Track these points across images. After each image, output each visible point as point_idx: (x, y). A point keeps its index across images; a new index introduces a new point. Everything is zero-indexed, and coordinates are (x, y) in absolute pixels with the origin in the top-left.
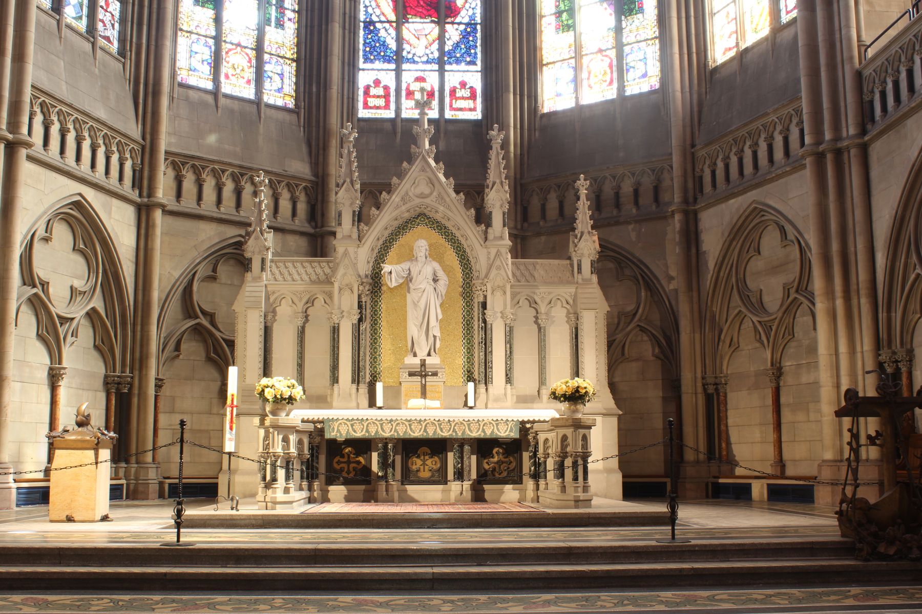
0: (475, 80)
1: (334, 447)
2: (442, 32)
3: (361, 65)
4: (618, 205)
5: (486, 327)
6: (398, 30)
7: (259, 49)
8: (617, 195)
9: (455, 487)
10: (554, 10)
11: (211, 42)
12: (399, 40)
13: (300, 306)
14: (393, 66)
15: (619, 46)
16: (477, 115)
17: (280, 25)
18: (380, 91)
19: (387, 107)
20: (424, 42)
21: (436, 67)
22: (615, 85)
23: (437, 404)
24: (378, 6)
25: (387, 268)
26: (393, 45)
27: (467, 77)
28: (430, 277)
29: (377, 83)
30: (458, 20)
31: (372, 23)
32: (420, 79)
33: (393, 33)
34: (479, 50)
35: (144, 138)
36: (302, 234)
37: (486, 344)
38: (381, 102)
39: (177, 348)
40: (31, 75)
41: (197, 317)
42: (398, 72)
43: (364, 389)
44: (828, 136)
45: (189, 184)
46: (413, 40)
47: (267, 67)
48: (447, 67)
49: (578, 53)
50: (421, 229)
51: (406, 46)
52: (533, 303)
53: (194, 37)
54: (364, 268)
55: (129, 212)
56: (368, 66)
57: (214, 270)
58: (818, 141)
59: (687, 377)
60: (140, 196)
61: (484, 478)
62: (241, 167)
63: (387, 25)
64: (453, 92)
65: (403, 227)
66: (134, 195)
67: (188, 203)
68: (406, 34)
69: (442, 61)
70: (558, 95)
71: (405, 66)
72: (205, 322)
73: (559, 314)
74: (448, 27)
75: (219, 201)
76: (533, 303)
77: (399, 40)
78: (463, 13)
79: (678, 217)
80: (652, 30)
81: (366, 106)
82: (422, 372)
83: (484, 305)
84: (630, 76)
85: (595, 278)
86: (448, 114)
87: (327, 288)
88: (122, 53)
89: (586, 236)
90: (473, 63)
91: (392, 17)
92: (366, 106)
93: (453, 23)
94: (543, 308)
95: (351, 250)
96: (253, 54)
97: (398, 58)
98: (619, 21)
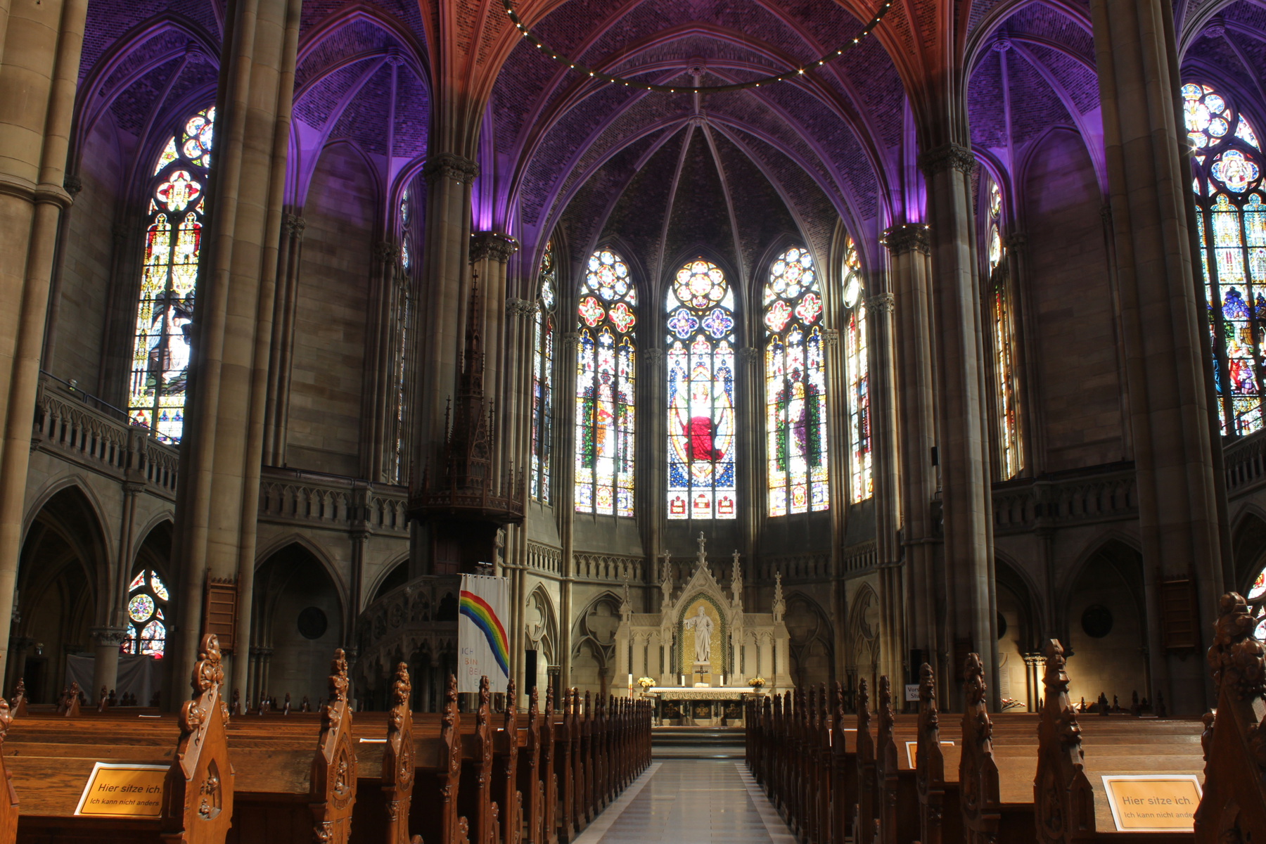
0: (733, 496)
1: (665, 703)
2: (714, 468)
3: (669, 488)
4: (807, 573)
5: (731, 648)
6: (689, 467)
7: (615, 486)
8: (806, 568)
9: (714, 719)
10: (775, 457)
11: (590, 486)
12: (690, 473)
13: (645, 637)
14: (686, 489)
15: (809, 482)
16: (733, 516)
17: (625, 470)
18: (680, 503)
19: (683, 512)
20: (703, 474)
21: (710, 489)
22: (806, 505)
23: (707, 685)
24: (678, 454)
25: (685, 621)
26: (686, 477)
27: (727, 494)
28: (705, 624)
29: (678, 498)
30: (722, 461)
31: (675, 464)
32: (702, 496)
33: (686, 469)
34: (734, 478)
35: (562, 546)
36: (639, 587)
37: (732, 654)
38: (680, 510)
39: (579, 650)
40: (527, 535)
41: (588, 635)
42: (690, 492)
43: (675, 676)
44: (886, 561)
45: (583, 566)
46: (698, 474)
47: (619, 495)
48: (717, 489)
50: (702, 601)
51: (694, 477)
52: (754, 634)
53: (582, 485)
54: (675, 620)
55: (556, 585)
56: (673, 489)
57: (595, 609)
58: (882, 562)
59: (837, 666)
60: (562, 576)
61: (726, 716)
62: (608, 554)
63: (683, 465)
64: (720, 503)
65: (693, 599)
66: (558, 576)
67: (583, 577)
68: (694, 470)
70: (778, 507)
71: (693, 489)
72: (592, 637)
73: (767, 639)
74: (717, 465)
75: (597, 574)
76: (754, 634)
77: (690, 473)
78: (725, 457)
79: (834, 583)
80: (825, 477)
81: (672, 512)
82: (701, 671)
83: (730, 637)
84: (815, 500)
85: (783, 623)
86: (718, 516)
87: (658, 628)
88: (551, 503)
89: (779, 602)
90: (731, 486)
91: (686, 460)
92: (672, 512)
93: (720, 463)
94: (758, 637)
95: (669, 612)
96: (611, 489)
97: (690, 484)
98: (809, 468)
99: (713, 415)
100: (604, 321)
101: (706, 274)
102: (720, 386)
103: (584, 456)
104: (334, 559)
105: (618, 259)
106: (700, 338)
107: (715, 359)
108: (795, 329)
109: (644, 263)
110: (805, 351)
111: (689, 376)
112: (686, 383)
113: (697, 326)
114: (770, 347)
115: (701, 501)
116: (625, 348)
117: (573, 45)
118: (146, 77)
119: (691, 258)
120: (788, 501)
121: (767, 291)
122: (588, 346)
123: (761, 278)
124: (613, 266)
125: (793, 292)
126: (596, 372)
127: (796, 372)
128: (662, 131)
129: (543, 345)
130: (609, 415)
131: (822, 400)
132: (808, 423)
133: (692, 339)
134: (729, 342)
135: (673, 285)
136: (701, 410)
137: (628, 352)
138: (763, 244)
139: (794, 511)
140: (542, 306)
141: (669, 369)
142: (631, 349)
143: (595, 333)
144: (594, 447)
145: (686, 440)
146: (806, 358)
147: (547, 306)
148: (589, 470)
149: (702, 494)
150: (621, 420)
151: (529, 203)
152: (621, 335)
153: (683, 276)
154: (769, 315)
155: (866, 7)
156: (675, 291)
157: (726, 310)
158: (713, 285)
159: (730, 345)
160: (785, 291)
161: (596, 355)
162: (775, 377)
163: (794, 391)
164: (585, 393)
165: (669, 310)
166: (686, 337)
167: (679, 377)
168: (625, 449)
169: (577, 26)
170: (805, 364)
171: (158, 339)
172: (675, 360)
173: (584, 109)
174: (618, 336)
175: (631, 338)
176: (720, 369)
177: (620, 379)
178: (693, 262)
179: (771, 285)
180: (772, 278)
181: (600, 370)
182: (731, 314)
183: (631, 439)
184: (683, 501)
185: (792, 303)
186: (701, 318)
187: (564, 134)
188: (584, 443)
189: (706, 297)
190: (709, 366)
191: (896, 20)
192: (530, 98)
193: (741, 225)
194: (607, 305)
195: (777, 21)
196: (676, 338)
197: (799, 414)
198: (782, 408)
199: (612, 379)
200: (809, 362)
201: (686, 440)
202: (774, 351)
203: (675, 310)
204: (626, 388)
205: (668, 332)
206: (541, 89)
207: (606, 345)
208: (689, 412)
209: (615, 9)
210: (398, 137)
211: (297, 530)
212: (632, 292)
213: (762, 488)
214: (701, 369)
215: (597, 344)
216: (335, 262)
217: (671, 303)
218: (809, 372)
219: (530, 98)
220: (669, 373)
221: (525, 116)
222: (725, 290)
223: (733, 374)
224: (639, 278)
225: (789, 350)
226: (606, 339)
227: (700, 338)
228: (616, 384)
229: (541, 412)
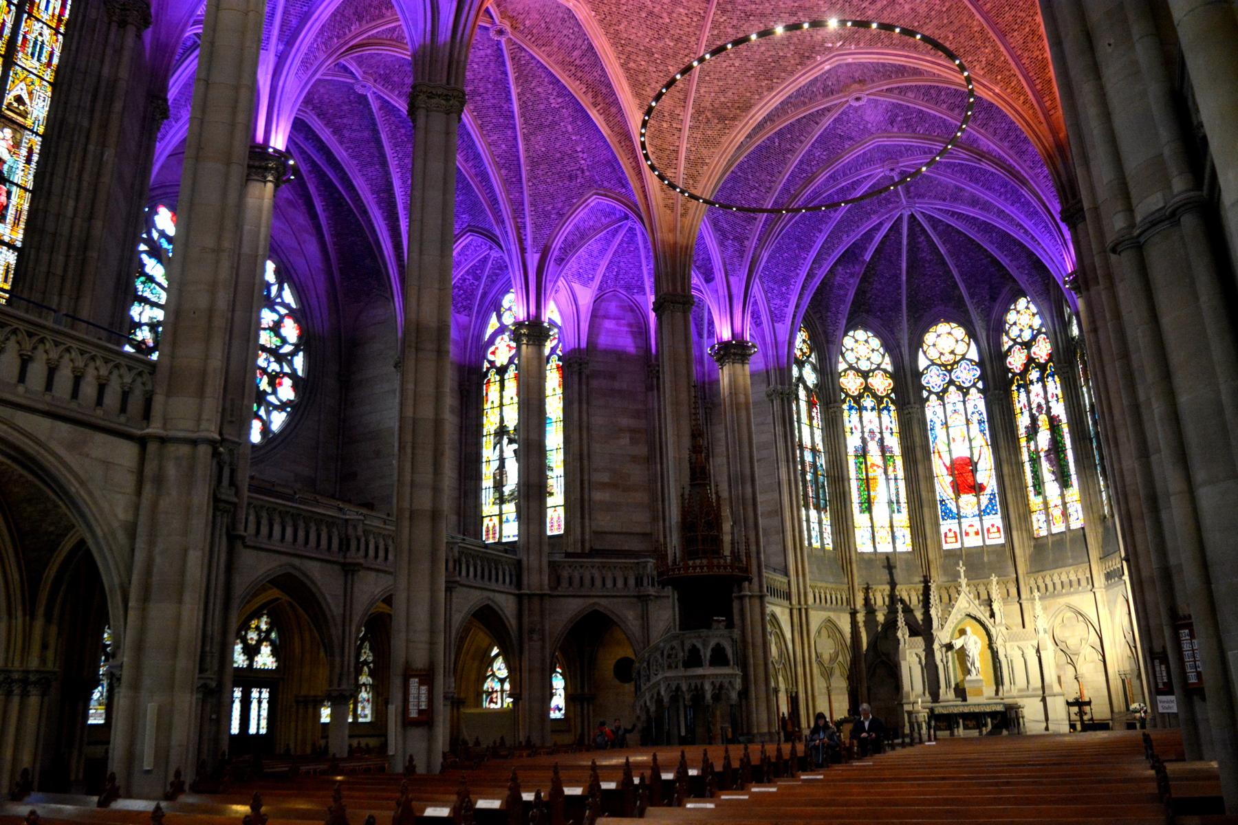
2: (979, 500)
3: (941, 522)
6: (957, 502)
12: (958, 507)
14: (956, 521)
15: (1064, 504)
17: (899, 511)
20: (970, 506)
21: (978, 518)
26: (955, 510)
29: (950, 530)
30: (986, 492)
33: (954, 504)
42: (960, 523)
46: (965, 507)
49: (1046, 503)
64: (988, 530)
68: (961, 504)
69: (981, 514)
71: (962, 520)
77: (958, 507)
86: (988, 542)
91: (953, 496)
96: (889, 529)
99: (972, 454)
100: (864, 389)
101: (950, 333)
102: (975, 428)
103: (861, 504)
105: (870, 334)
106: (952, 389)
107: (967, 405)
108: (1033, 368)
109: (892, 332)
110: (1044, 387)
111: (946, 423)
112: (945, 430)
113: (947, 379)
114: (1014, 388)
115: (971, 531)
116: (887, 408)
118: (467, 272)
119: (935, 322)
120: (1048, 521)
121: (1005, 338)
122: (853, 411)
123: (998, 328)
124: (866, 341)
125: (1027, 336)
126: (863, 432)
127: (1039, 406)
128: (881, 224)
129: (811, 418)
130: (879, 467)
131: (1065, 429)
132: (1056, 448)
133: (945, 391)
134: (978, 389)
135: (922, 347)
136: (961, 451)
137: (889, 411)
138: (993, 299)
139: (1055, 530)
140: (806, 387)
141: (928, 420)
142: (892, 407)
143: (857, 399)
144: (869, 495)
145: (951, 479)
146: (1046, 392)
147: (811, 387)
148: (867, 515)
149: (970, 522)
150: (890, 469)
152: (882, 398)
153: (929, 338)
154: (1009, 359)
155: (994, 93)
156: (925, 353)
157: (971, 361)
158: (957, 341)
159: (979, 390)
160: (1020, 336)
161: (861, 417)
162: (1022, 413)
163: (1040, 423)
164: (856, 451)
165: (921, 369)
166: (939, 390)
167: (938, 426)
168: (897, 494)
170: (1046, 398)
171: (498, 462)
172: (933, 410)
174: (879, 400)
175: (891, 399)
176: (973, 413)
177: (884, 435)
178: (936, 325)
179: (1007, 334)
180: (1007, 326)
181: (866, 430)
182: (977, 364)
183: (902, 485)
184: (955, 533)
185: (1027, 345)
186: (950, 372)
188: (860, 494)
189: (952, 352)
190: (962, 411)
191: (1022, 98)
193: (968, 287)
194: (865, 375)
195: (941, 118)
196: (930, 392)
197: (1047, 443)
198: (1032, 439)
199: (879, 436)
200: (1049, 395)
201: (951, 479)
202: (1018, 390)
203: (927, 368)
204: (893, 442)
205: (924, 388)
207: (869, 408)
208: (950, 454)
209: (801, 142)
211: (596, 600)
212: (887, 359)
213: (1026, 513)
214: (956, 415)
215: (861, 409)
216: (617, 385)
217: (922, 363)
218: (1051, 404)
220: (929, 423)
221: (746, 243)
222: (969, 345)
223: (985, 415)
224: (890, 347)
225: (1031, 387)
226: (868, 402)
227: (952, 389)
228: (882, 440)
229: (815, 474)
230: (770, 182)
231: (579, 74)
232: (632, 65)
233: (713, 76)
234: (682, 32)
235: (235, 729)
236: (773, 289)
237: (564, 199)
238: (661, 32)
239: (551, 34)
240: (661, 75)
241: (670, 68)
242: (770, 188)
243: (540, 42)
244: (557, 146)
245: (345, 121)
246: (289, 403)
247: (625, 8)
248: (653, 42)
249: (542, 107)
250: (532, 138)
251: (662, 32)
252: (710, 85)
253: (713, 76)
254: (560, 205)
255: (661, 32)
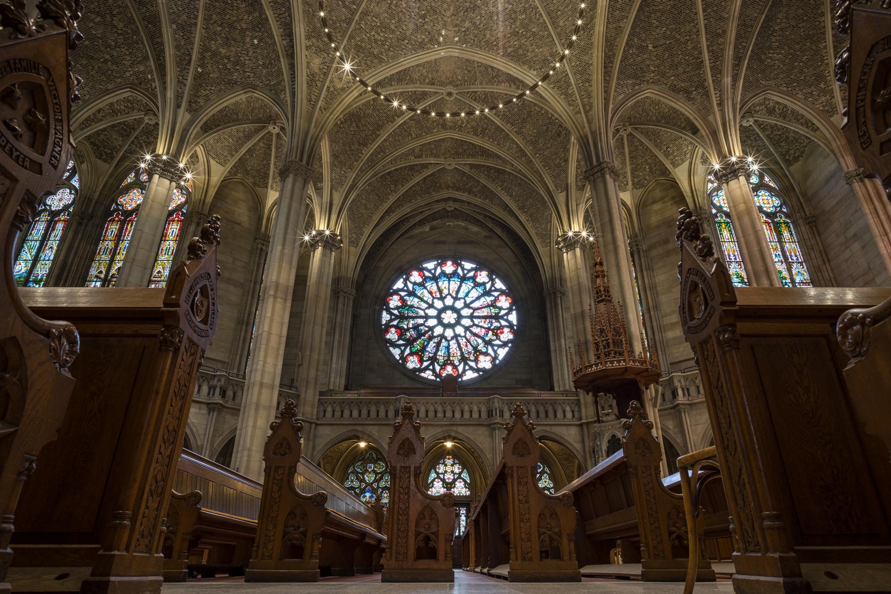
104: (669, 429)
117: (696, 22)
151: (824, 104)
169: (687, 11)
173: (805, 18)
187: (808, 44)
192: (701, 72)
206: (702, 62)
210: (671, 157)
219: (701, 72)
221: (706, 84)
230: (695, 27)
231: (500, 79)
232: (509, 50)
233: (562, 8)
234: (523, 4)
235: (457, 534)
236: (811, 93)
237: (562, 150)
238: (513, 17)
239: (473, 72)
240: (531, 39)
241: (533, 30)
242: (698, 31)
243: (473, 81)
244: (541, 123)
245: (470, 184)
246: (509, 341)
247: (482, 25)
248: (513, 26)
249: (516, 110)
250: (524, 130)
251: (513, 16)
252: (565, 15)
253: (562, 8)
254: (563, 155)
255: (513, 17)
